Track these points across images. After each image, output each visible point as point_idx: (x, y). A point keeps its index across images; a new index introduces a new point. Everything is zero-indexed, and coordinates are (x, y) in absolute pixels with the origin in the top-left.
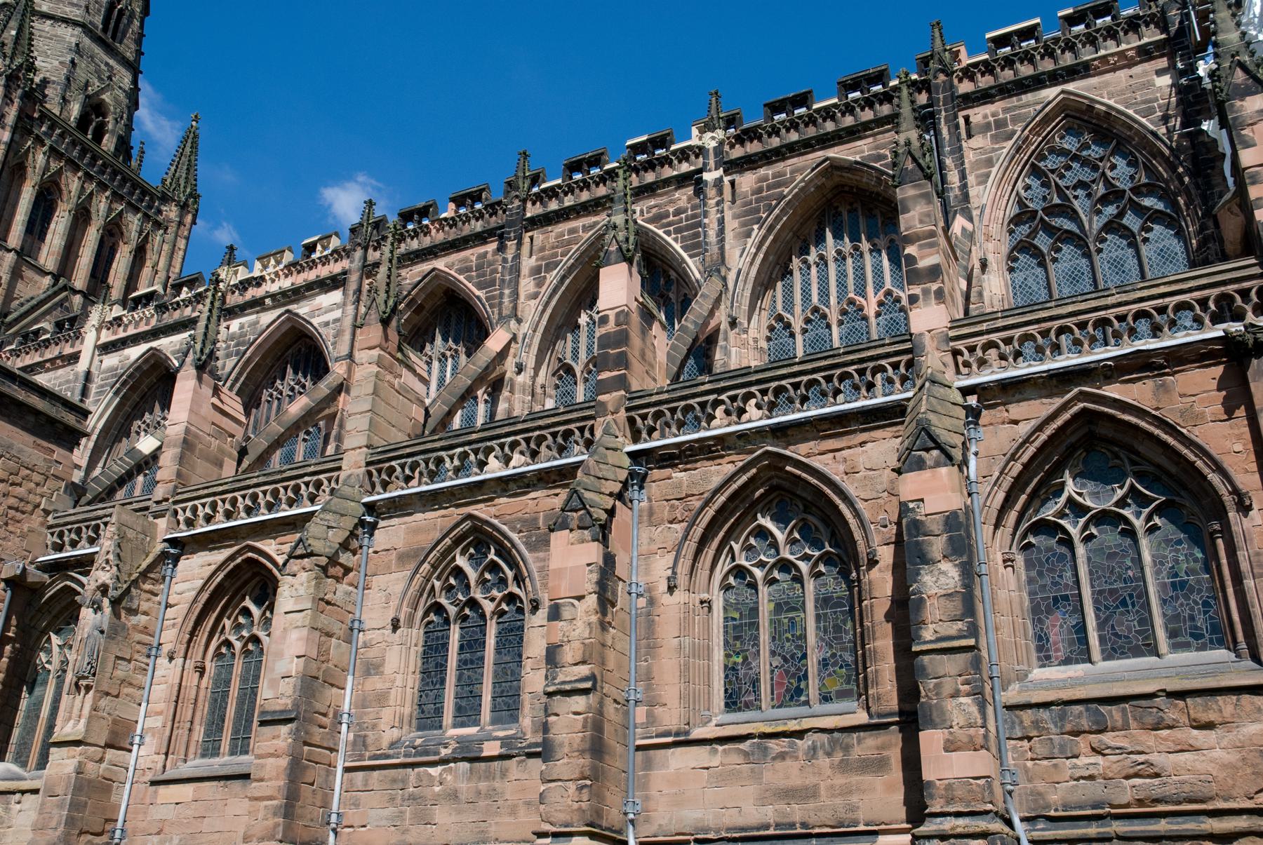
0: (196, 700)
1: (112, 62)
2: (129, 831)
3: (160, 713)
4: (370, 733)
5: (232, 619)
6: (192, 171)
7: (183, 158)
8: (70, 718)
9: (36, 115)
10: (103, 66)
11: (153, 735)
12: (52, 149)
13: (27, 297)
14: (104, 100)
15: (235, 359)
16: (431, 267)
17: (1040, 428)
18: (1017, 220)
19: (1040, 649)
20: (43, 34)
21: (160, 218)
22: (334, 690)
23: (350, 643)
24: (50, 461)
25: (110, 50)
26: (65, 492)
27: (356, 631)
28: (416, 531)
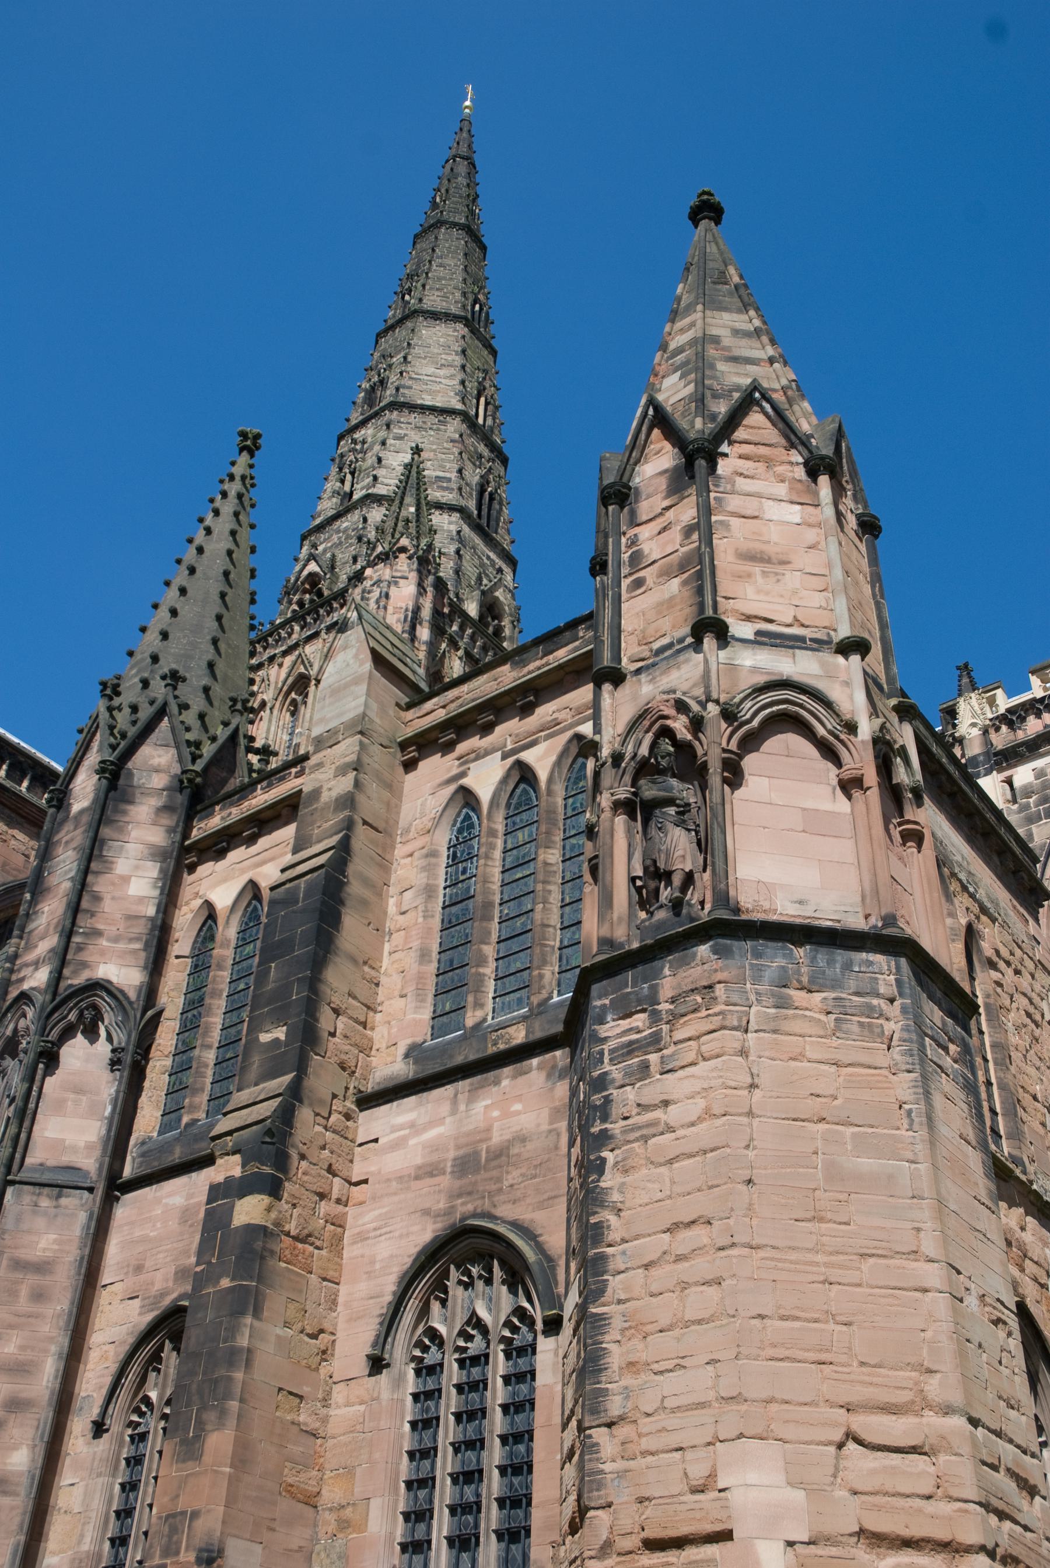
1: (492, 555)
9: (446, 610)
10: (486, 561)
14: (498, 598)
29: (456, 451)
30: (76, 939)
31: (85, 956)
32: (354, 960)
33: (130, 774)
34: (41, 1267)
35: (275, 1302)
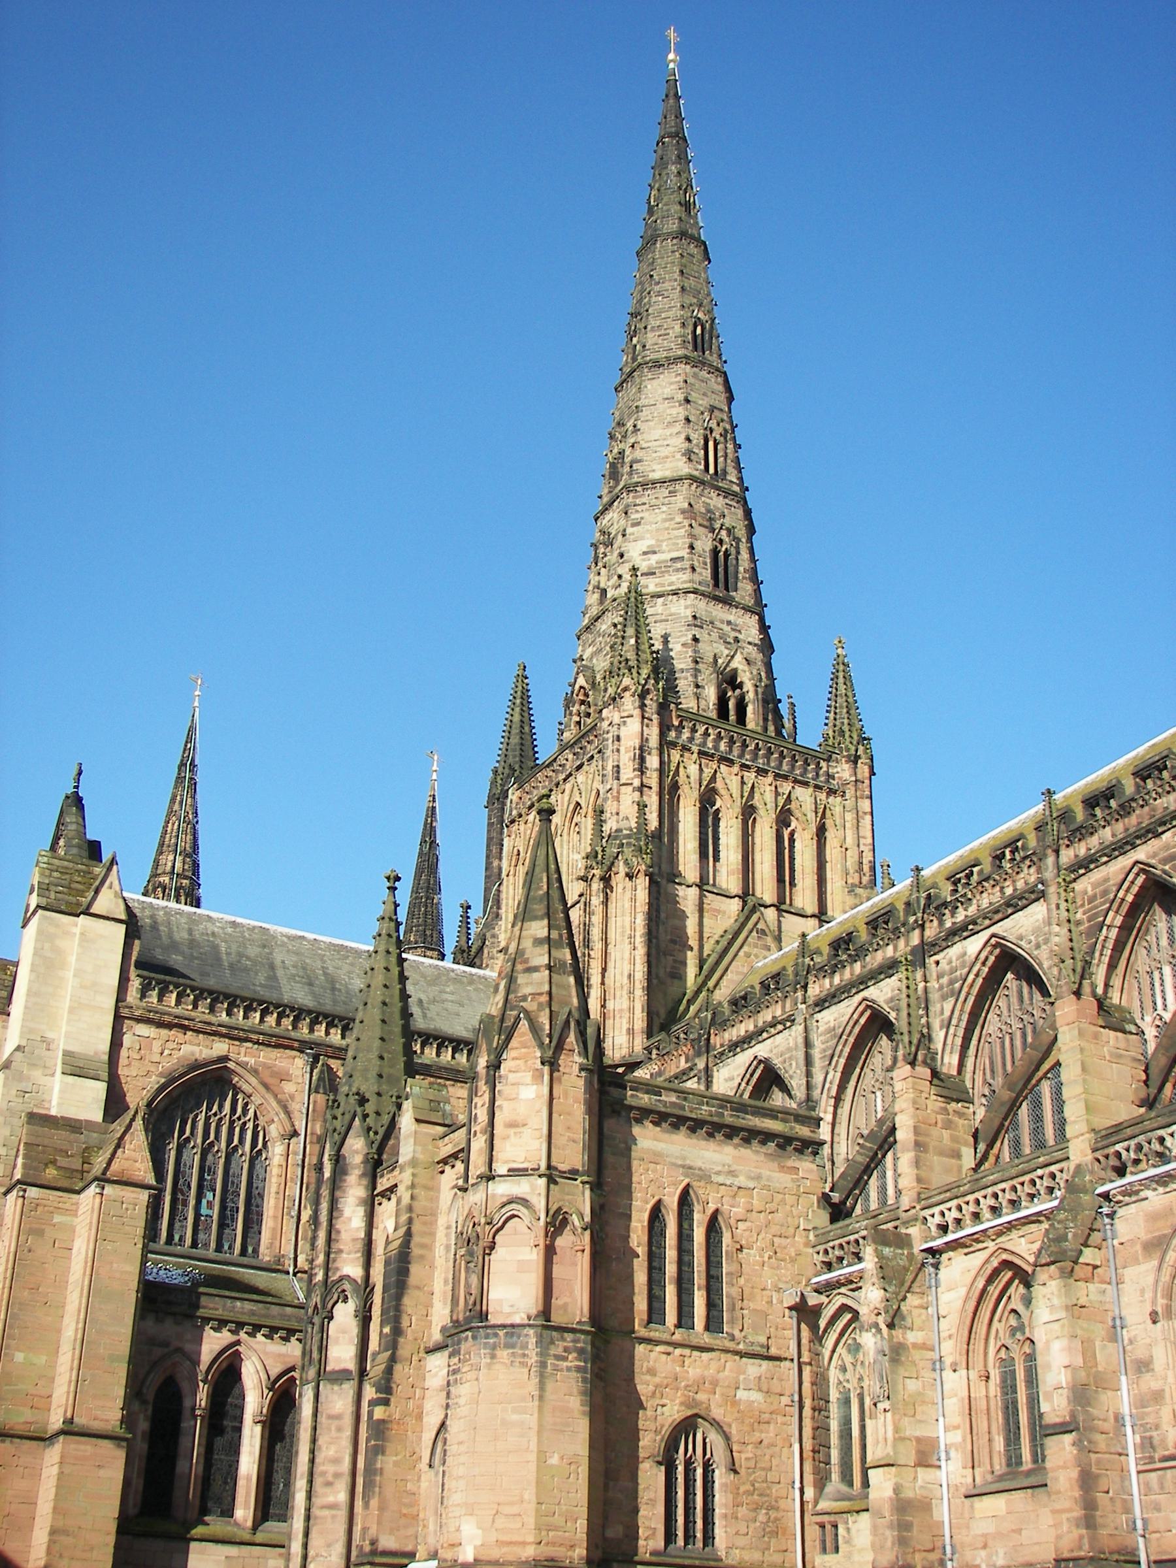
0: (988, 1409)
2: (958, 1547)
3: (957, 1427)
4: (1154, 1434)
5: (1004, 1318)
6: (852, 712)
7: (839, 700)
8: (878, 1442)
10: (727, 628)
11: (957, 1450)
12: (700, 753)
13: (721, 932)
15: (952, 1000)
16: (1131, 861)
20: (658, 618)
21: (834, 783)
22: (1110, 1393)
23: (1116, 1341)
24: (798, 1180)
25: (727, 602)
26: (819, 1207)
27: (1119, 1329)
28: (1154, 1217)
29: (686, 523)
30: (332, 1256)
31: (337, 1264)
32: (418, 1288)
33: (345, 1158)
34: (338, 1417)
35: (390, 1447)
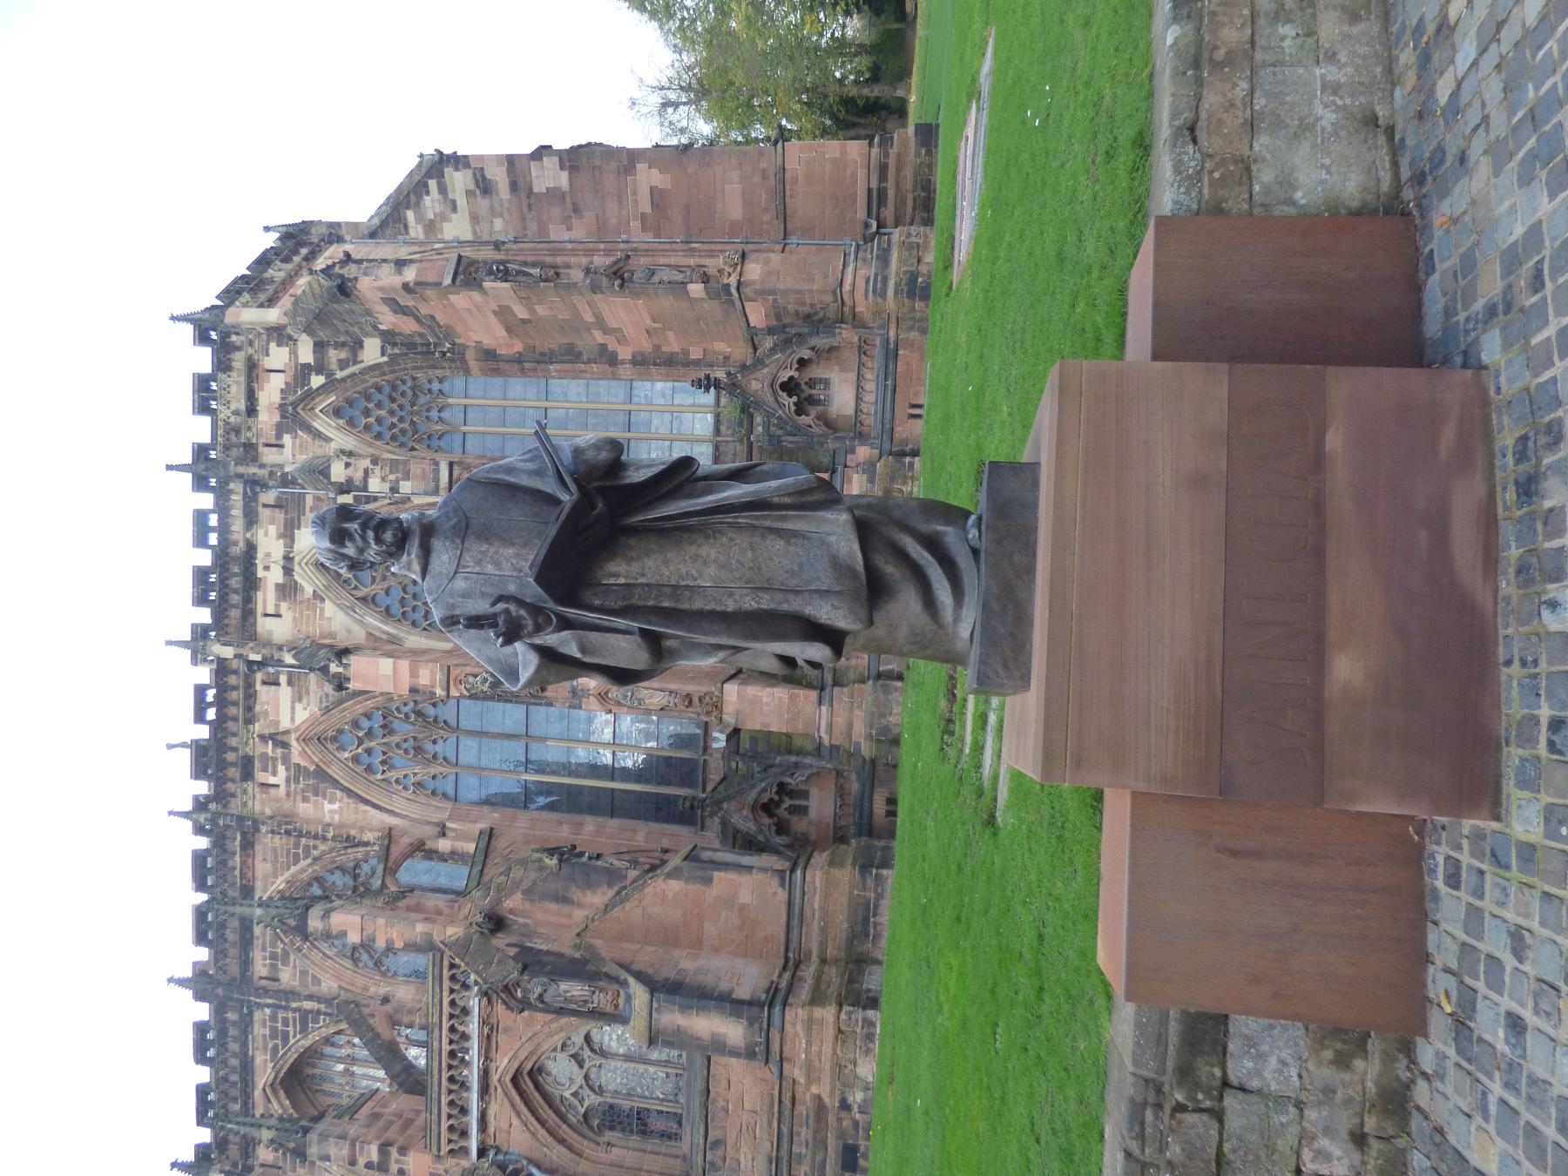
17: (518, 1114)
18: (355, 961)
19: (669, 1137)
